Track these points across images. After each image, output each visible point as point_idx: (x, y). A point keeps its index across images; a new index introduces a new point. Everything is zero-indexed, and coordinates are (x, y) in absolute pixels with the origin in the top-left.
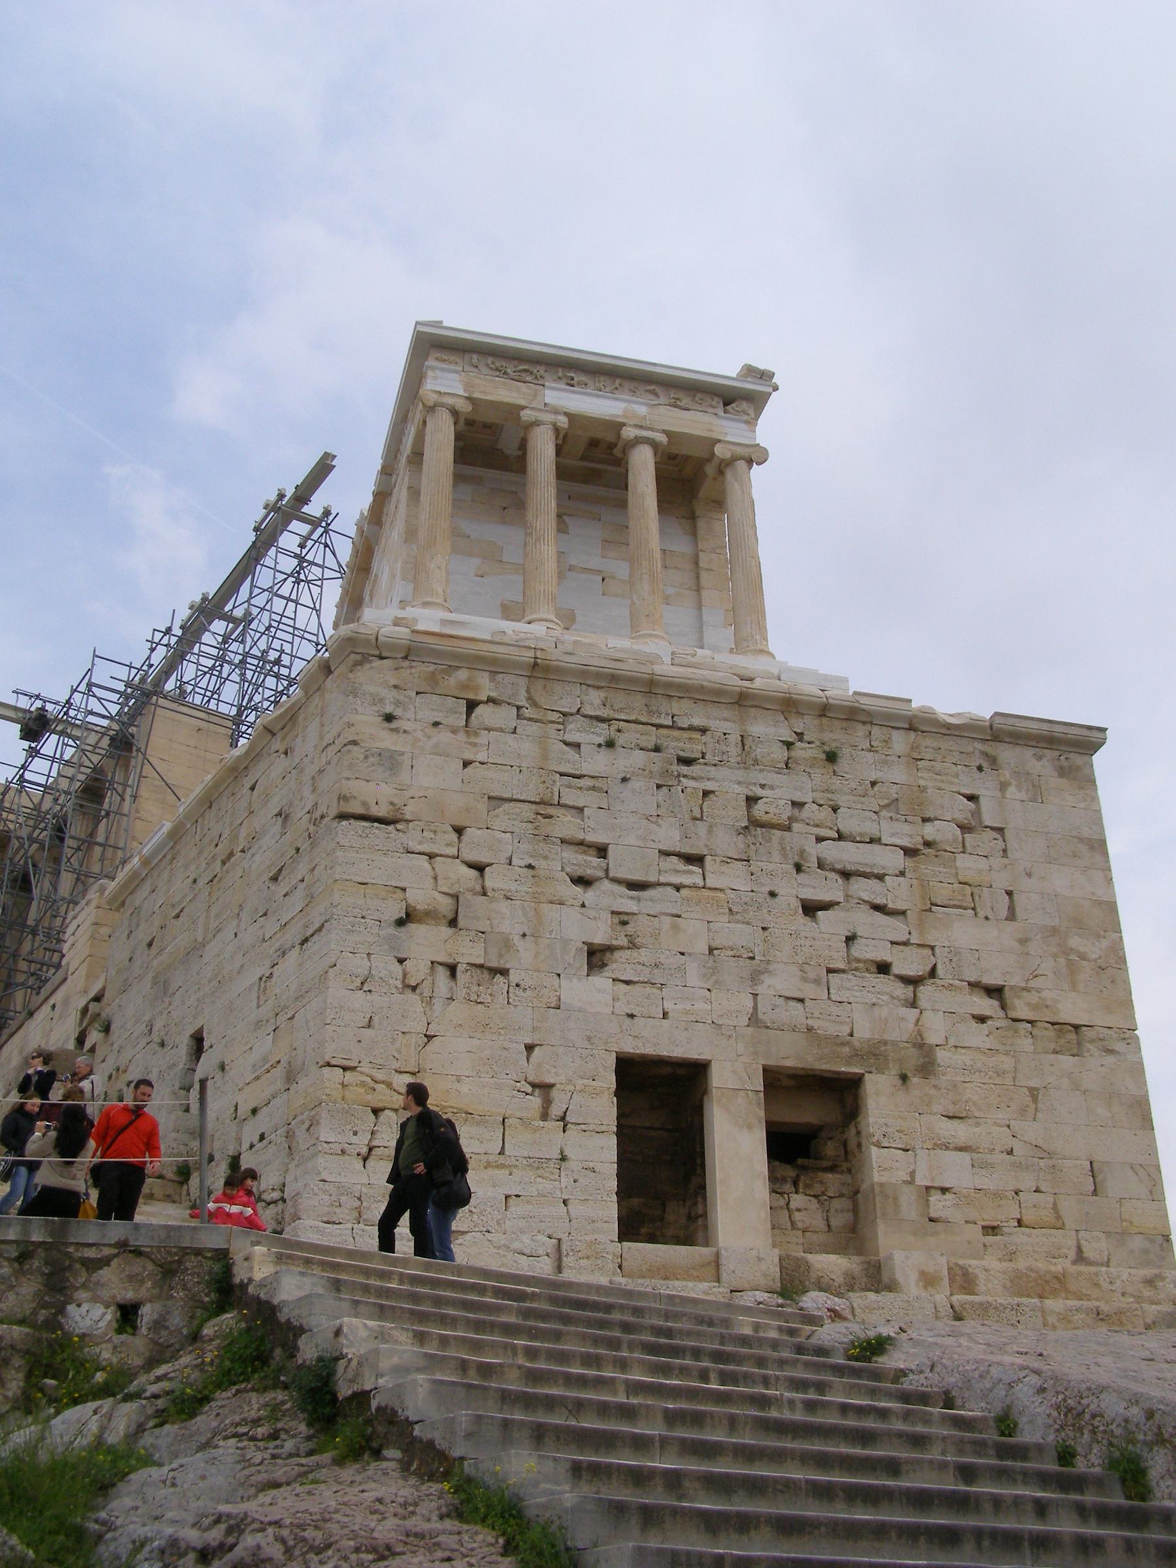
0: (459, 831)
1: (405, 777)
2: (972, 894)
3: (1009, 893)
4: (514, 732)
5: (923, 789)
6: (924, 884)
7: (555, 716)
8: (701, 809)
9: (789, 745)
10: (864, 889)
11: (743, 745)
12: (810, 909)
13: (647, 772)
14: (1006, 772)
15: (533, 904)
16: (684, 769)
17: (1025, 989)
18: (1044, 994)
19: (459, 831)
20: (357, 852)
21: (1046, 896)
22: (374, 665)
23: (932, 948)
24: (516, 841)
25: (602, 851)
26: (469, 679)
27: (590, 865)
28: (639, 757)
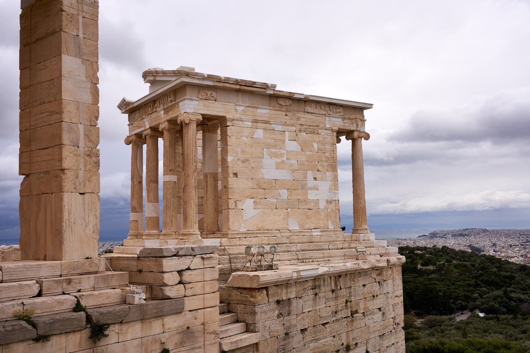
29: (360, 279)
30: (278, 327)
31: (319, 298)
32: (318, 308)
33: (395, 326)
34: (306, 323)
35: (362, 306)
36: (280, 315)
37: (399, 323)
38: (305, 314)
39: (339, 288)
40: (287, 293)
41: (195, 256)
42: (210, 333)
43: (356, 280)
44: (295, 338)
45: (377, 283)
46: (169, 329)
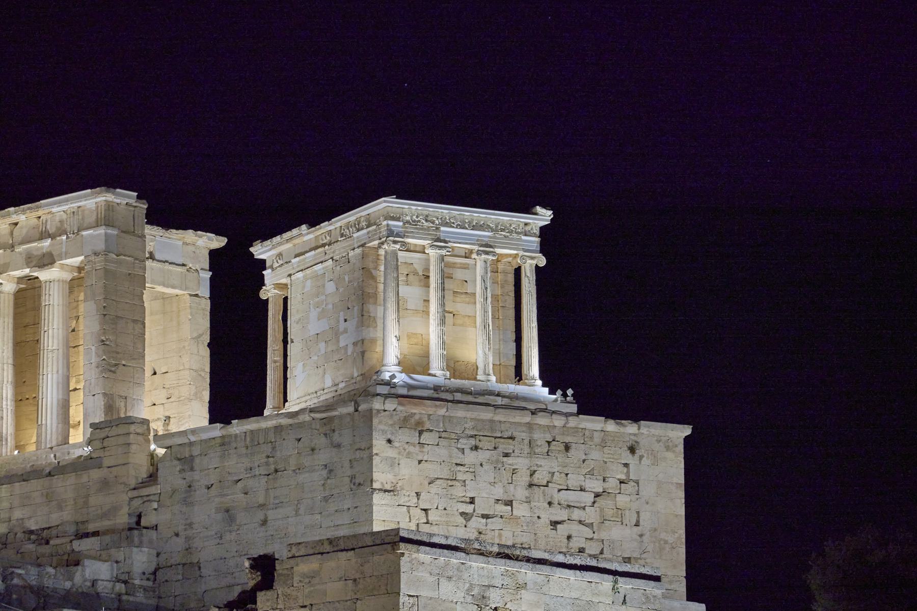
0: (418, 494)
1: (396, 469)
2: (622, 514)
3: (638, 513)
4: (438, 445)
5: (606, 463)
6: (602, 510)
7: (453, 436)
8: (512, 478)
9: (549, 443)
10: (577, 514)
11: (530, 444)
12: (555, 524)
13: (490, 461)
14: (643, 450)
15: (446, 527)
16: (505, 459)
17: (640, 559)
18: (647, 561)
19: (418, 494)
20: (381, 506)
21: (653, 513)
22: (382, 414)
23: (603, 540)
24: (439, 498)
25: (472, 501)
26: (420, 419)
27: (469, 509)
28: (487, 454)
29: (290, 431)
30: (180, 484)
31: (229, 454)
32: (226, 464)
33: (352, 486)
34: (213, 479)
35: (293, 462)
36: (182, 471)
37: (362, 482)
38: (211, 470)
39: (256, 443)
40: (190, 451)
41: (113, 426)
42: (121, 483)
43: (283, 433)
44: (198, 492)
45: (322, 435)
46: (93, 479)
